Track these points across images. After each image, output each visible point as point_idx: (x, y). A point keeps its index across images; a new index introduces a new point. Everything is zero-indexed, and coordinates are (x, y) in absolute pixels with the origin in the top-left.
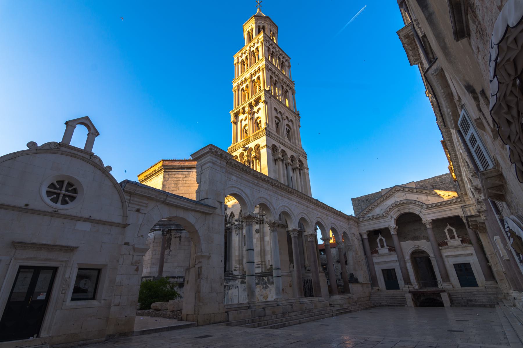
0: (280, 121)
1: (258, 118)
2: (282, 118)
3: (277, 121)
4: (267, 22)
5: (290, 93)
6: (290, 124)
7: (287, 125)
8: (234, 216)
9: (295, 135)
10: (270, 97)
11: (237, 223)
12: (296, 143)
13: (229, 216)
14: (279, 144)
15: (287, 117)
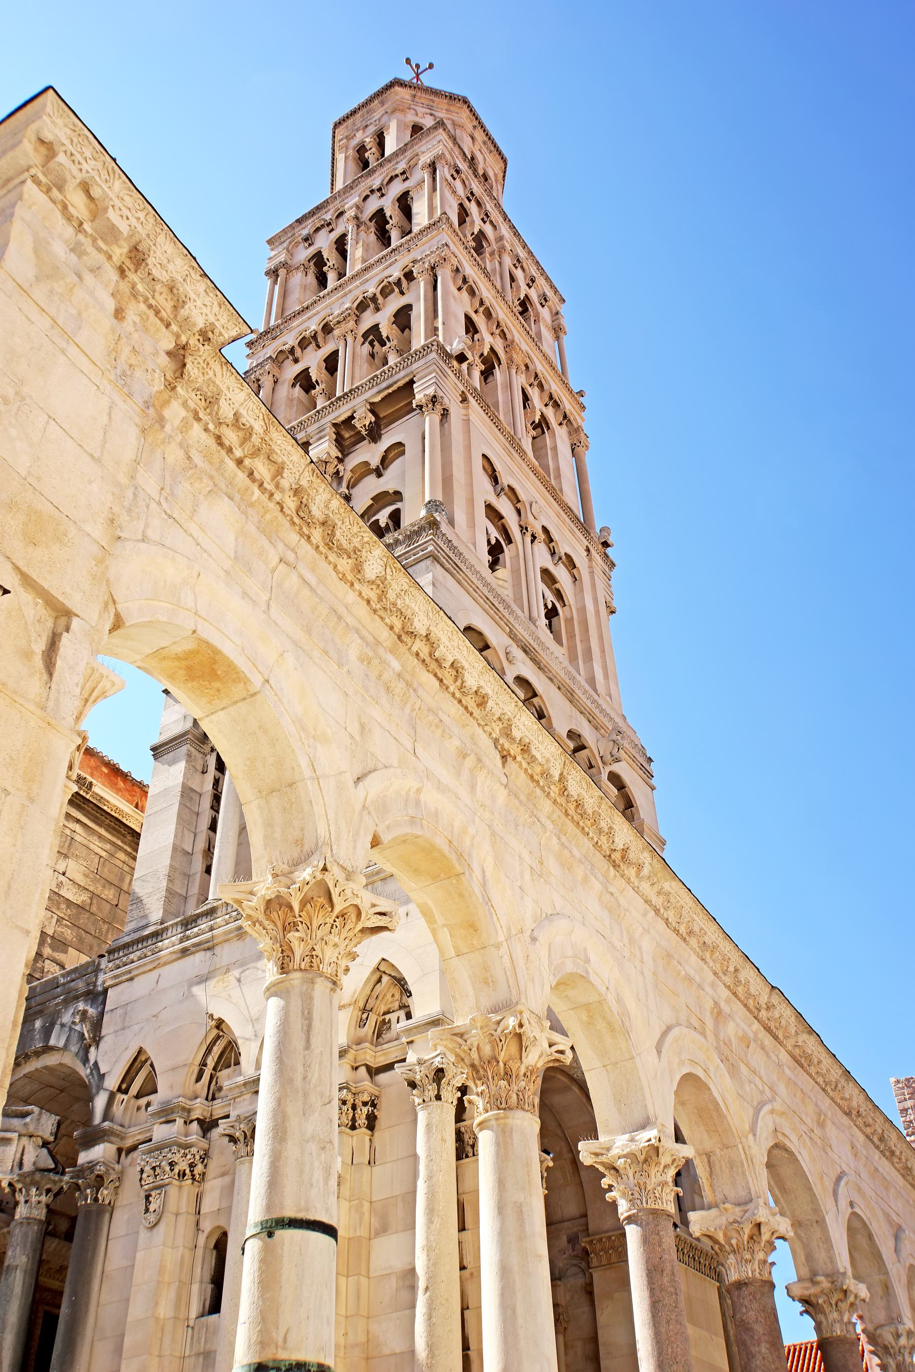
0: (509, 541)
1: (381, 499)
2: (523, 529)
3: (495, 534)
4: (463, 116)
5: (561, 435)
6: (561, 573)
7: (548, 576)
8: (150, 1088)
9: (586, 639)
10: (464, 400)
11: (160, 1132)
12: (592, 681)
13: (112, 1082)
14: (510, 642)
15: (545, 530)
